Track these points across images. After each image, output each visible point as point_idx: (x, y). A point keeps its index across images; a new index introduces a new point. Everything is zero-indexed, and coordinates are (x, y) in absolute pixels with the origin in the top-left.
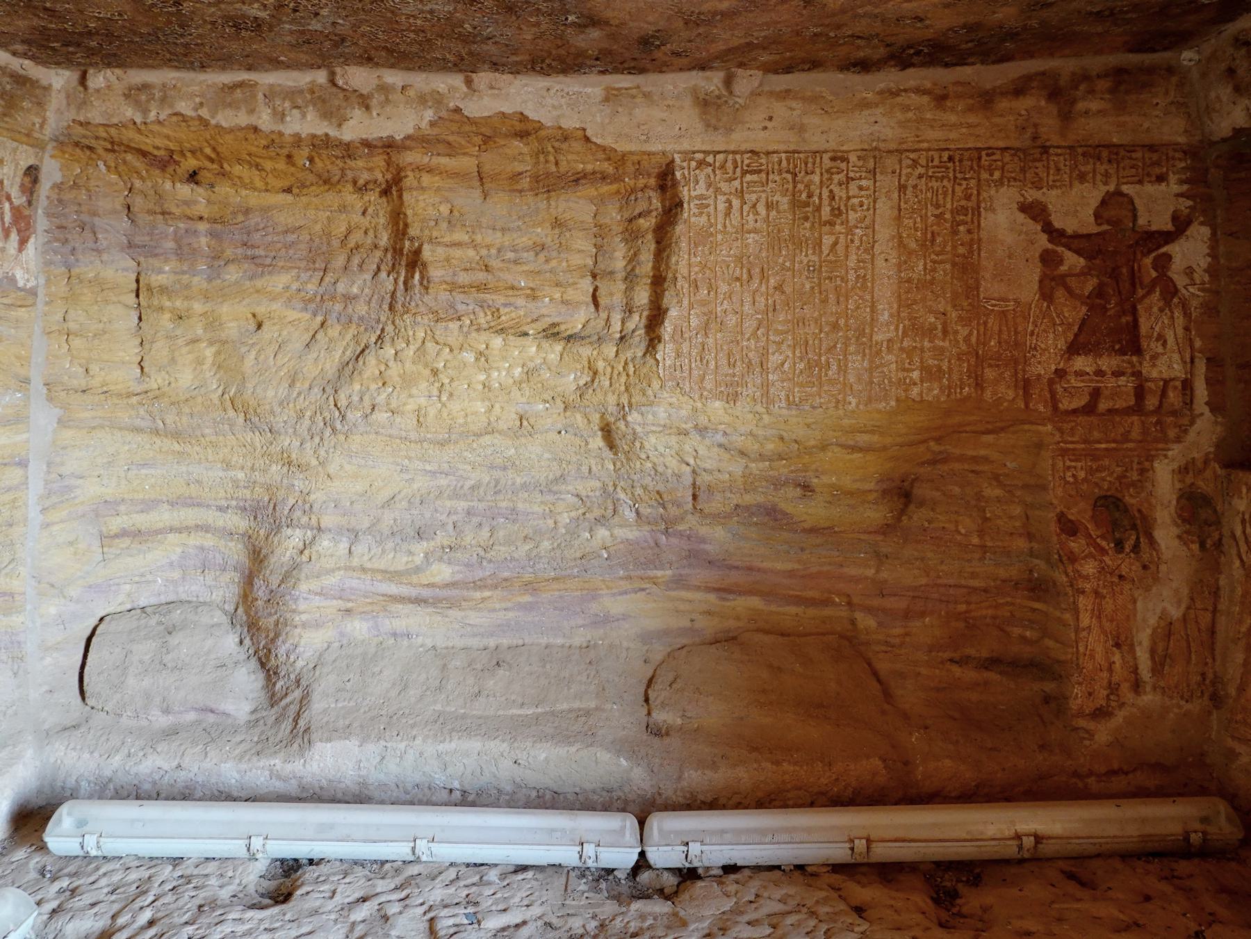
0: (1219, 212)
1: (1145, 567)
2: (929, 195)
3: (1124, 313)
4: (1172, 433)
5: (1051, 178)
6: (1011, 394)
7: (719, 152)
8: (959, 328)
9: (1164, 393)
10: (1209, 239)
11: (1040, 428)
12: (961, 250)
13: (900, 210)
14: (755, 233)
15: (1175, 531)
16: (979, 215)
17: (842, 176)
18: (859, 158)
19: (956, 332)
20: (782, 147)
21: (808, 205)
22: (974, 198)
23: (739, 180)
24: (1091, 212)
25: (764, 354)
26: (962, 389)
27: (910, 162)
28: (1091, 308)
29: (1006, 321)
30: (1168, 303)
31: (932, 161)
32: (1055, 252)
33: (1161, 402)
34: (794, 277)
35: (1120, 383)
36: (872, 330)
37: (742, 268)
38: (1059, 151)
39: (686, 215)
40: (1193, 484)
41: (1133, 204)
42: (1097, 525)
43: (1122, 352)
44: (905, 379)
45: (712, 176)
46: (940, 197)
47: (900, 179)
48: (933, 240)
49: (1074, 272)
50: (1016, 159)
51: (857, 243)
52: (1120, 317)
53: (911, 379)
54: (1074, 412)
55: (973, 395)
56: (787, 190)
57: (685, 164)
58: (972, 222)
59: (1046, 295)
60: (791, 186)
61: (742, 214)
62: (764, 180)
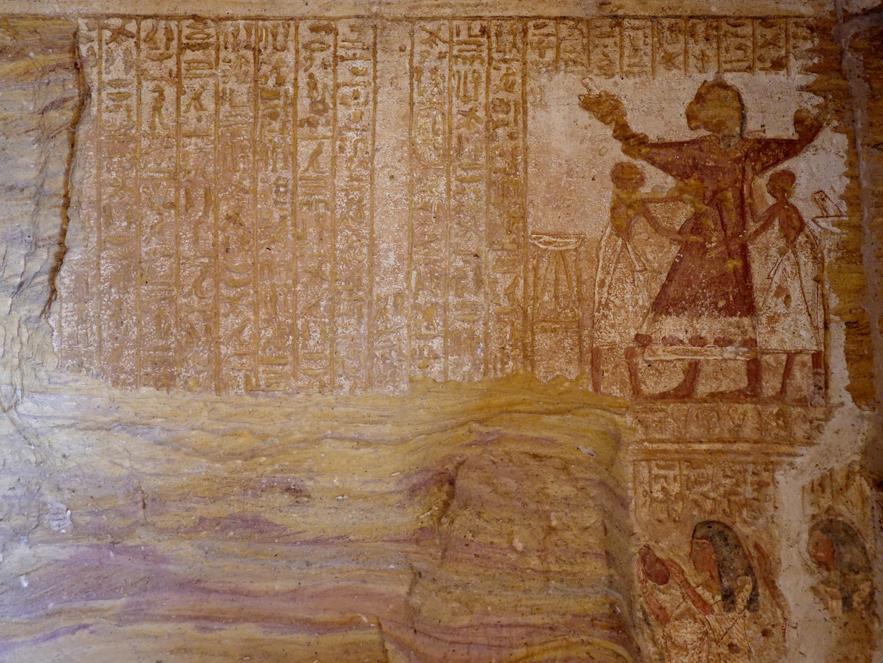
0: (859, 113)
2: (454, 82)
3: (730, 255)
4: (800, 430)
5: (626, 61)
6: (573, 371)
7: (146, 17)
8: (498, 276)
9: (787, 373)
10: (848, 152)
12: (500, 163)
13: (412, 104)
14: (198, 136)
16: (525, 113)
17: (327, 55)
18: (352, 29)
19: (495, 282)
20: (240, 11)
21: (277, 96)
22: (517, 88)
23: (174, 58)
24: (682, 111)
25: (212, 318)
26: (504, 364)
27: (426, 36)
28: (686, 247)
29: (566, 266)
30: (791, 242)
31: (458, 35)
32: (633, 167)
33: (784, 385)
34: (256, 201)
35: (726, 355)
36: (372, 280)
37: (177, 189)
38: (637, 23)
39: (94, 110)
41: (740, 100)
43: (729, 311)
44: (422, 351)
45: (134, 52)
46: (470, 86)
47: (411, 61)
48: (459, 151)
49: (660, 196)
50: (577, 32)
51: (349, 152)
52: (725, 261)
53: (431, 350)
54: (663, 396)
55: (521, 372)
56: (246, 73)
57: (94, 34)
58: (516, 121)
59: (623, 230)
60: (251, 69)
61: (178, 108)
62: (213, 59)
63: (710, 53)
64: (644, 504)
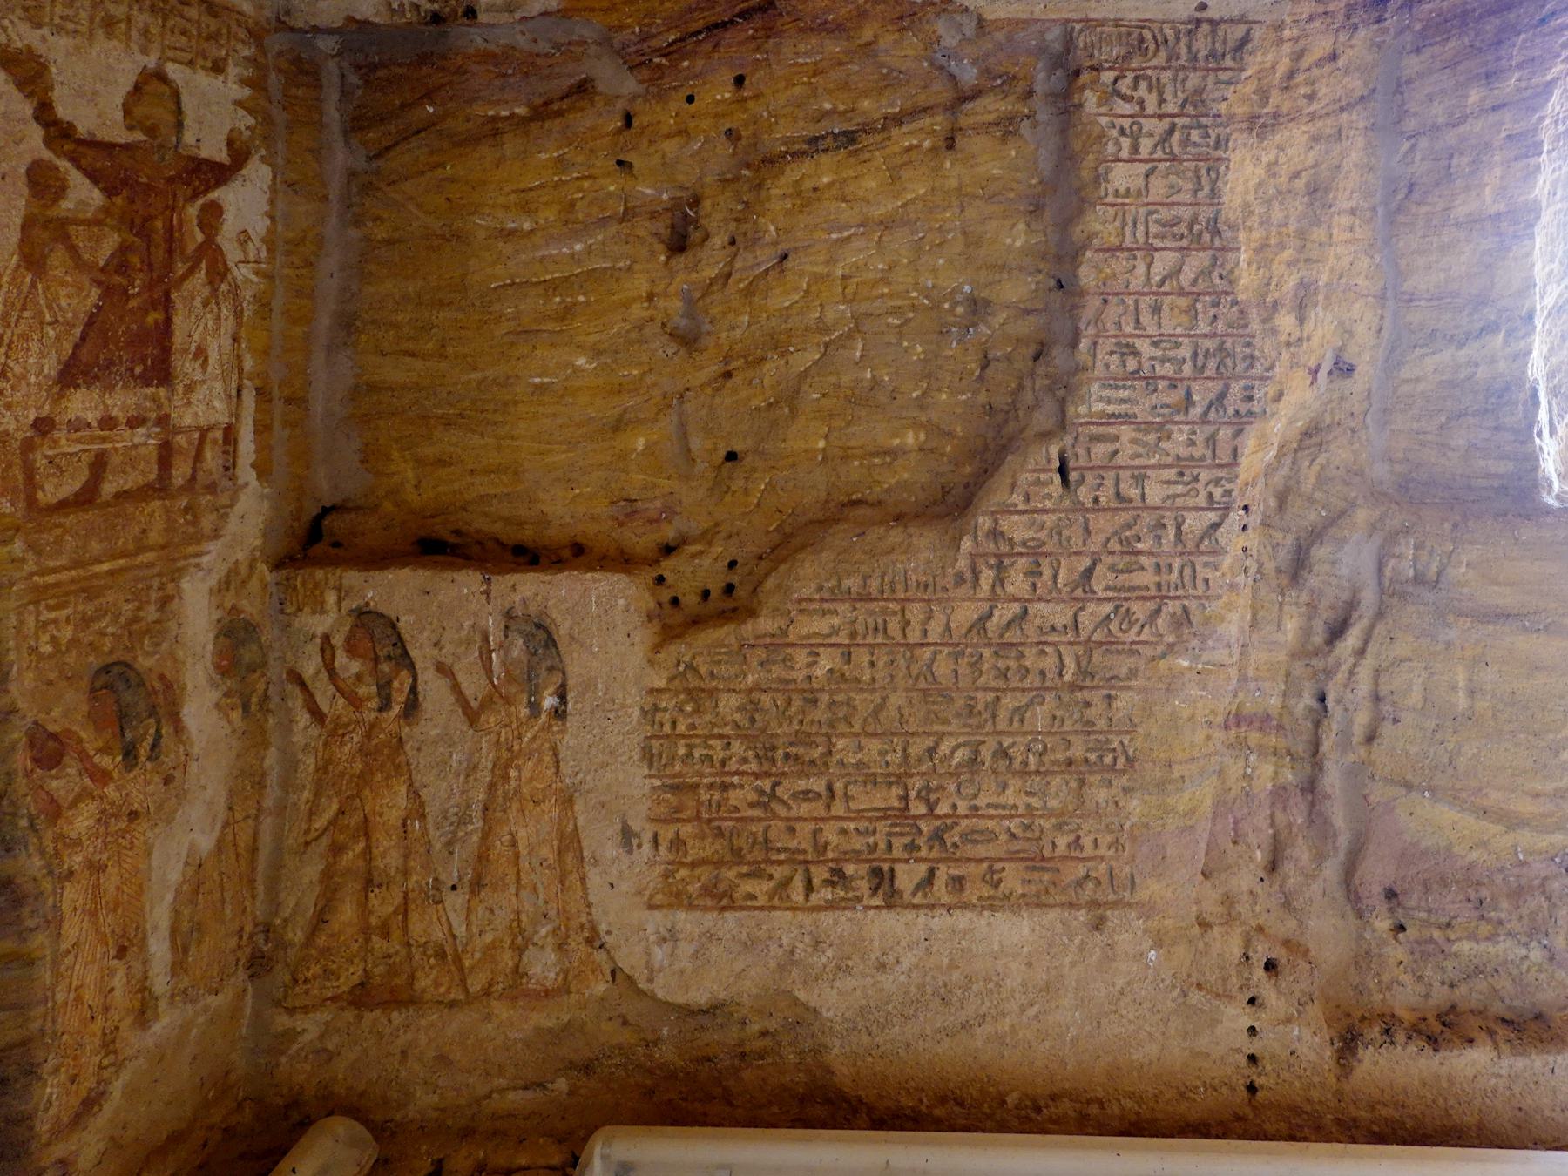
3: (154, 305)
9: (198, 457)
24: (119, 101)
28: (108, 291)
40: (234, 608)
41: (178, 104)
43: (145, 381)
49: (81, 216)
52: (146, 312)
59: (32, 260)
63: (154, 30)
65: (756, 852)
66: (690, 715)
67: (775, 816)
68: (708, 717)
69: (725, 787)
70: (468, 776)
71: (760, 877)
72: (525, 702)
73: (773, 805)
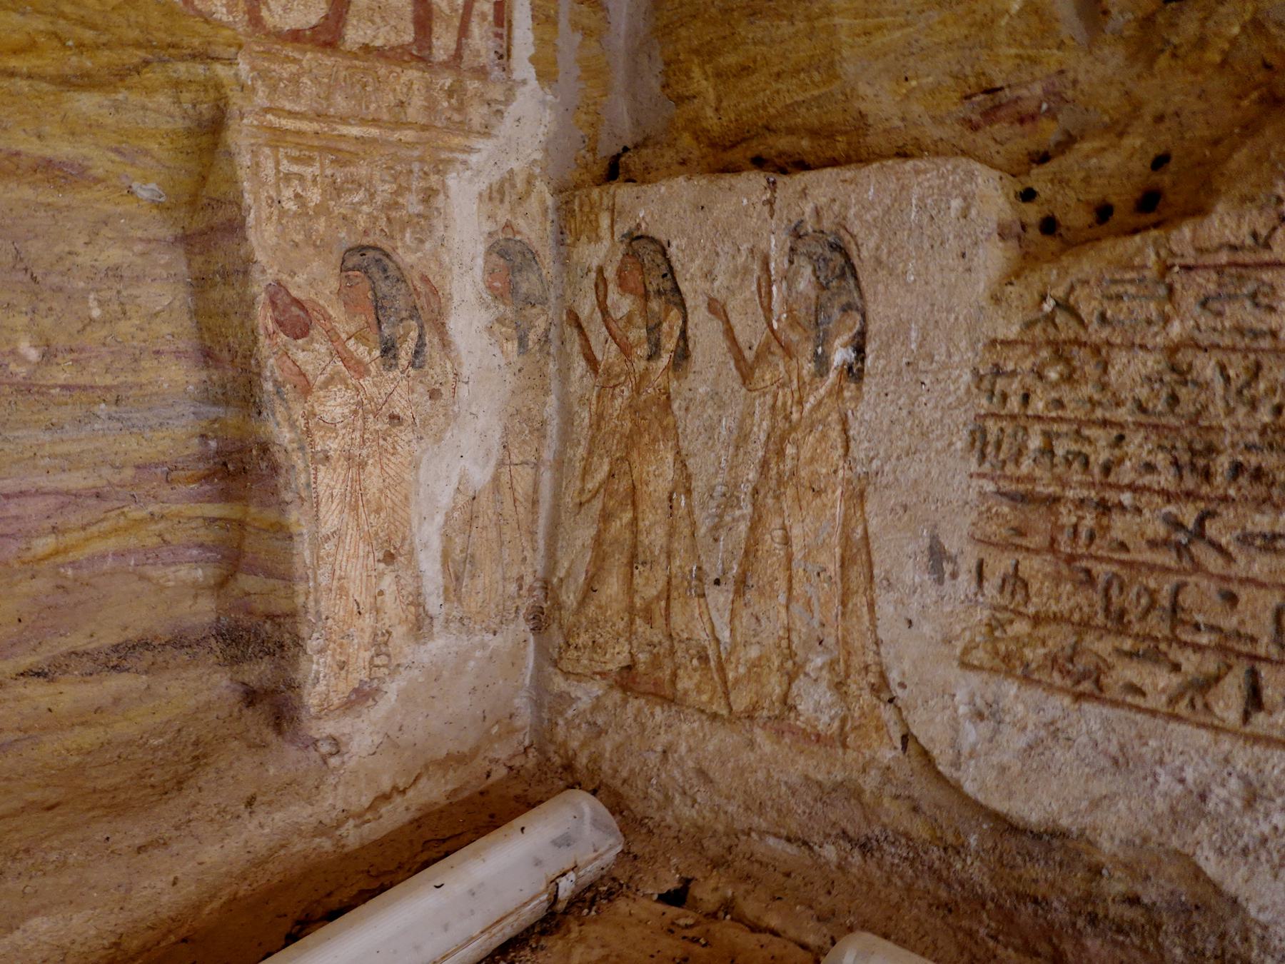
1: (434, 394)
11: (220, 70)
15: (483, 317)
40: (508, 225)
42: (352, 315)
54: (296, 36)
64: (269, 218)
65: (1153, 619)
66: (1055, 385)
67: (1197, 567)
68: (1088, 390)
69: (1104, 508)
70: (737, 448)
71: (1156, 662)
72: (809, 355)
73: (1199, 550)
